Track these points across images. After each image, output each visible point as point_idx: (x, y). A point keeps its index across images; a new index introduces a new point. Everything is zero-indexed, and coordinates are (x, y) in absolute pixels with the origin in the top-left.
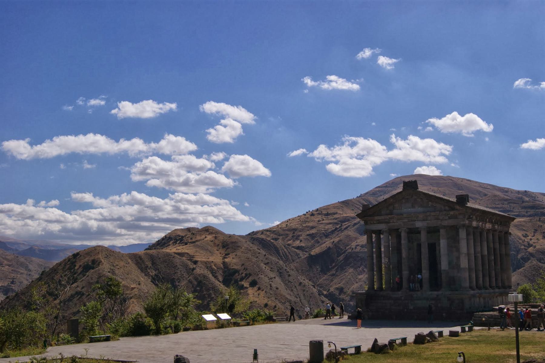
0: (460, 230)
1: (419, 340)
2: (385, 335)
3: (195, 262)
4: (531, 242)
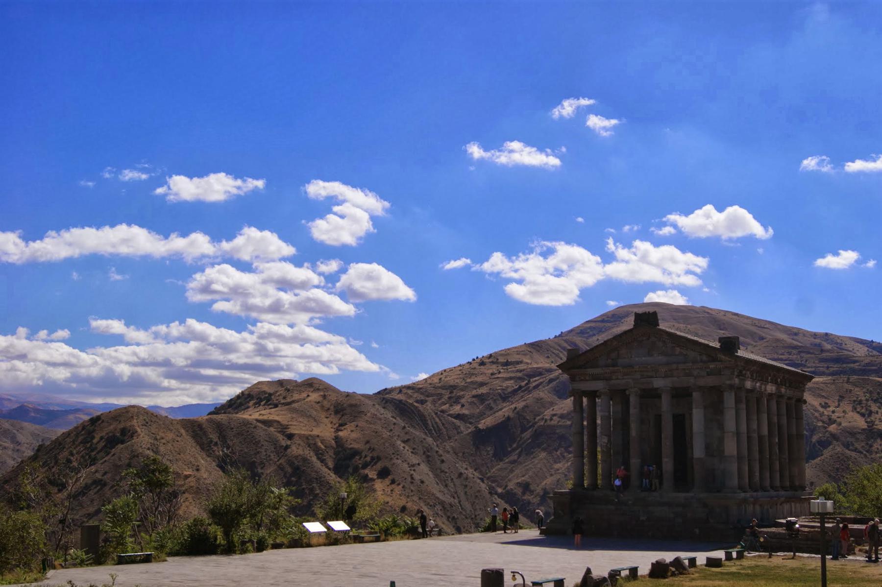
0: (725, 394)
1: (659, 570)
2: (603, 561)
3: (290, 437)
4: (834, 416)
